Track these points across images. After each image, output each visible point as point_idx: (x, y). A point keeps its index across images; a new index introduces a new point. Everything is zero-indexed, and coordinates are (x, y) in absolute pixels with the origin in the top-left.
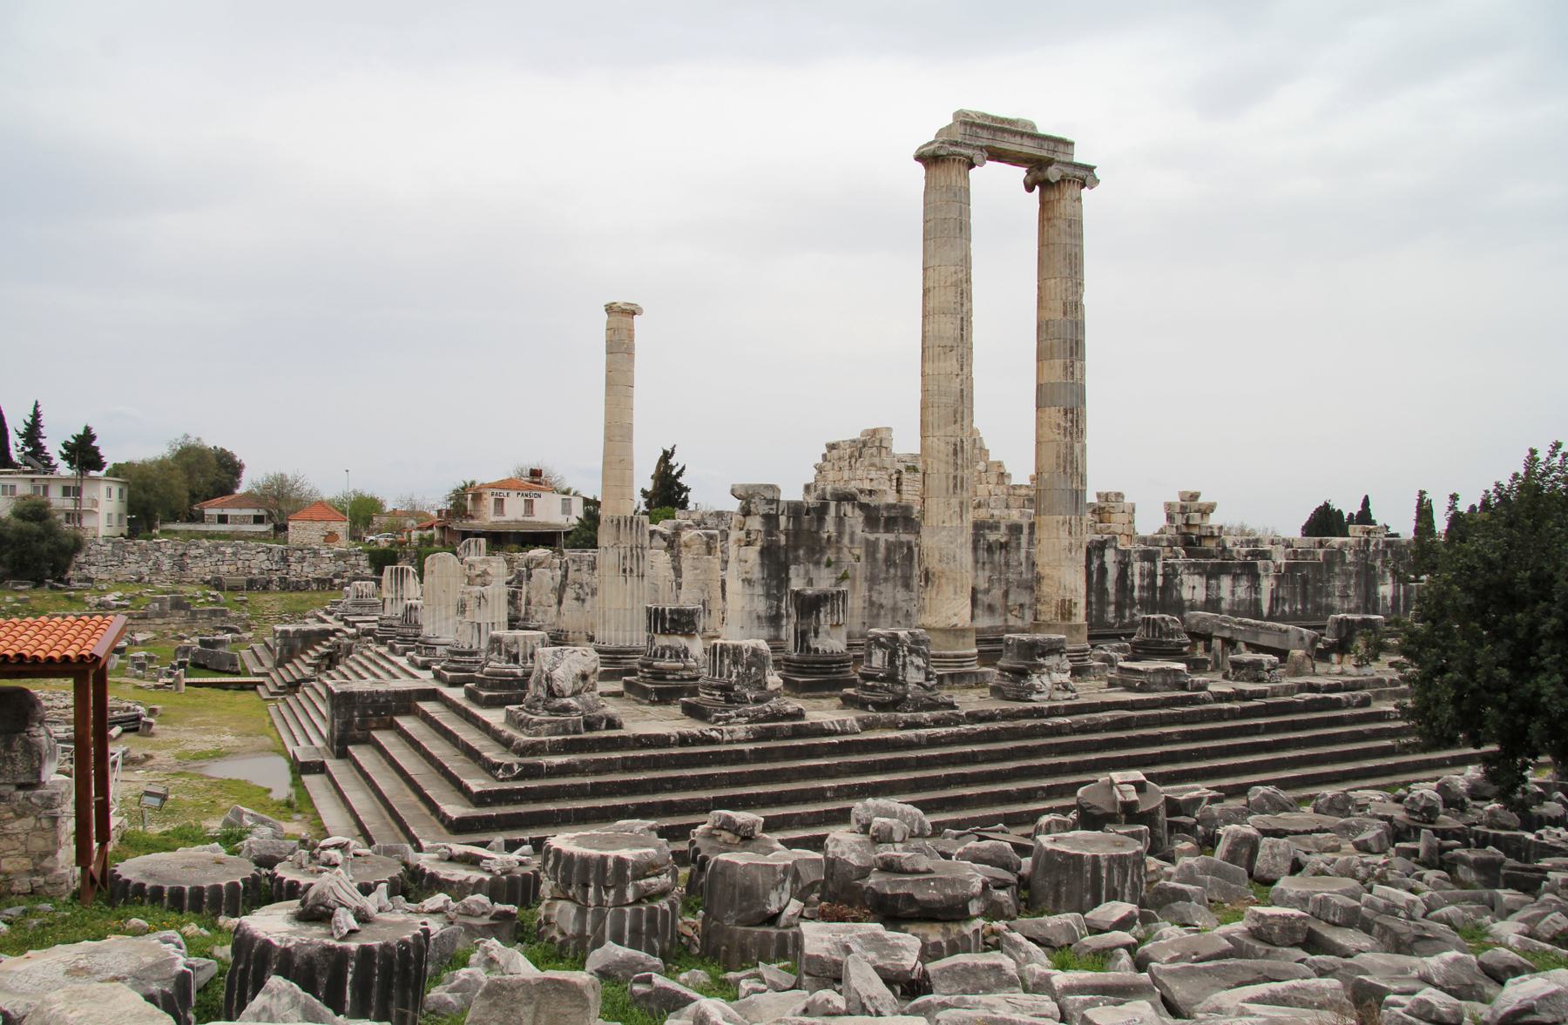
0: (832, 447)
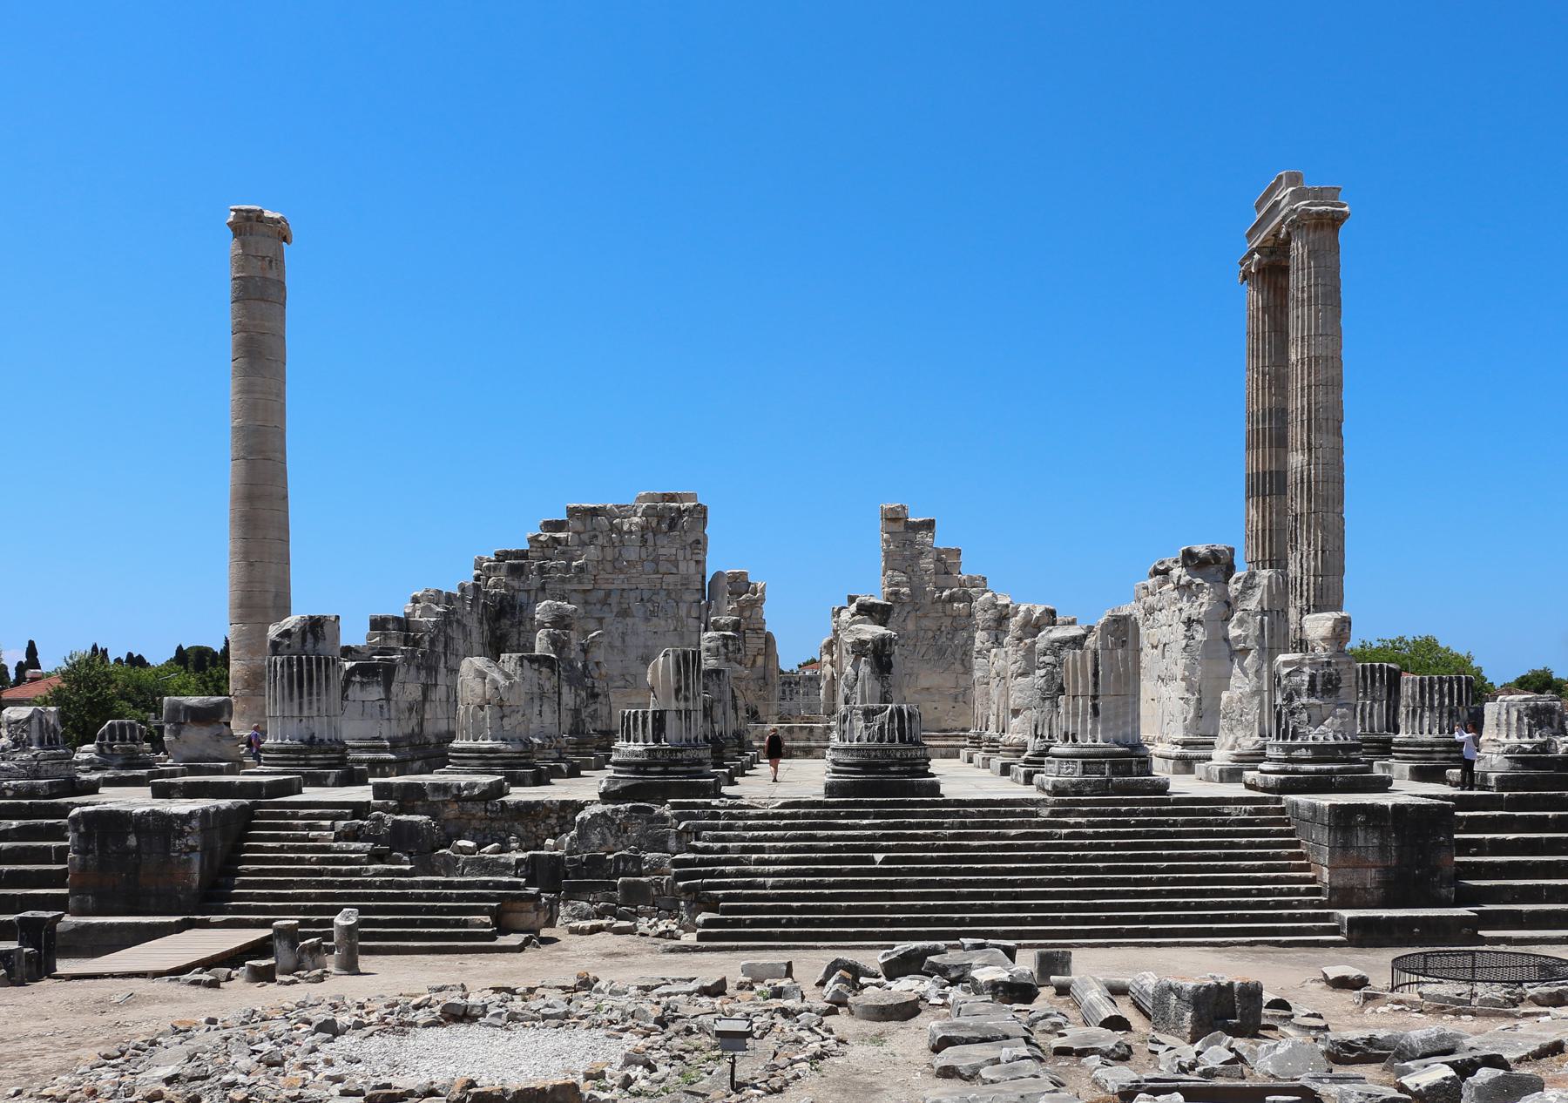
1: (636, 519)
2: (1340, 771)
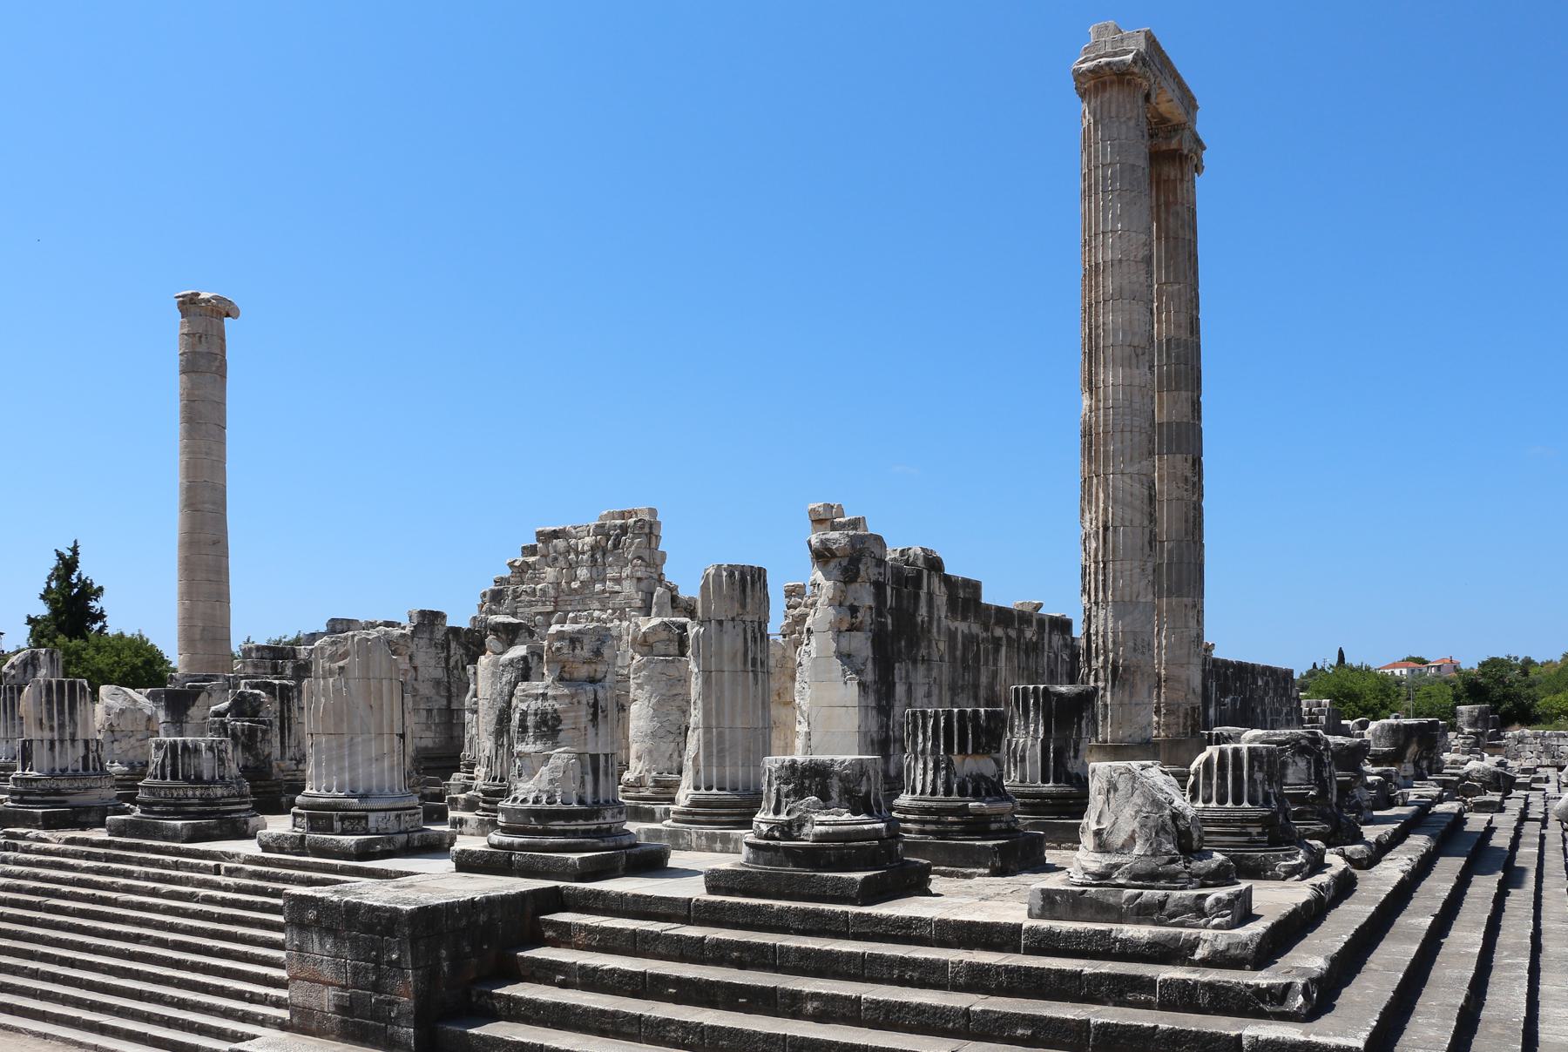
0: (547, 537)
1: (587, 539)
2: (522, 847)
